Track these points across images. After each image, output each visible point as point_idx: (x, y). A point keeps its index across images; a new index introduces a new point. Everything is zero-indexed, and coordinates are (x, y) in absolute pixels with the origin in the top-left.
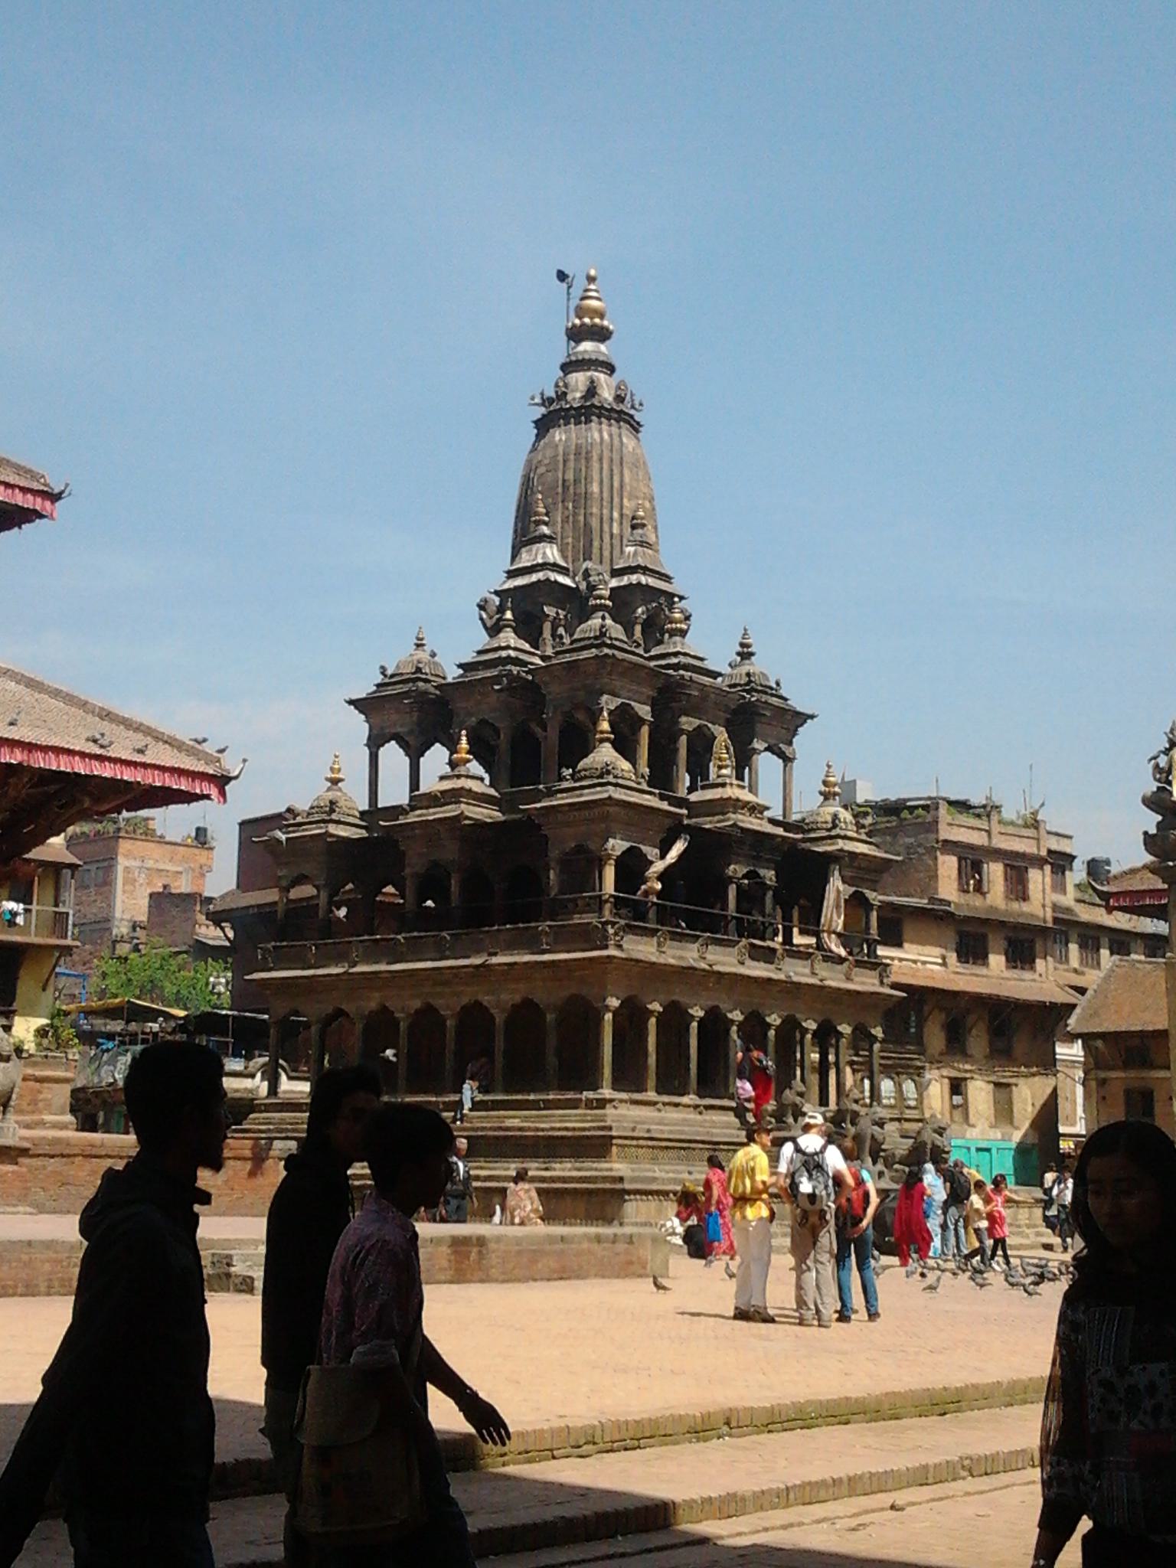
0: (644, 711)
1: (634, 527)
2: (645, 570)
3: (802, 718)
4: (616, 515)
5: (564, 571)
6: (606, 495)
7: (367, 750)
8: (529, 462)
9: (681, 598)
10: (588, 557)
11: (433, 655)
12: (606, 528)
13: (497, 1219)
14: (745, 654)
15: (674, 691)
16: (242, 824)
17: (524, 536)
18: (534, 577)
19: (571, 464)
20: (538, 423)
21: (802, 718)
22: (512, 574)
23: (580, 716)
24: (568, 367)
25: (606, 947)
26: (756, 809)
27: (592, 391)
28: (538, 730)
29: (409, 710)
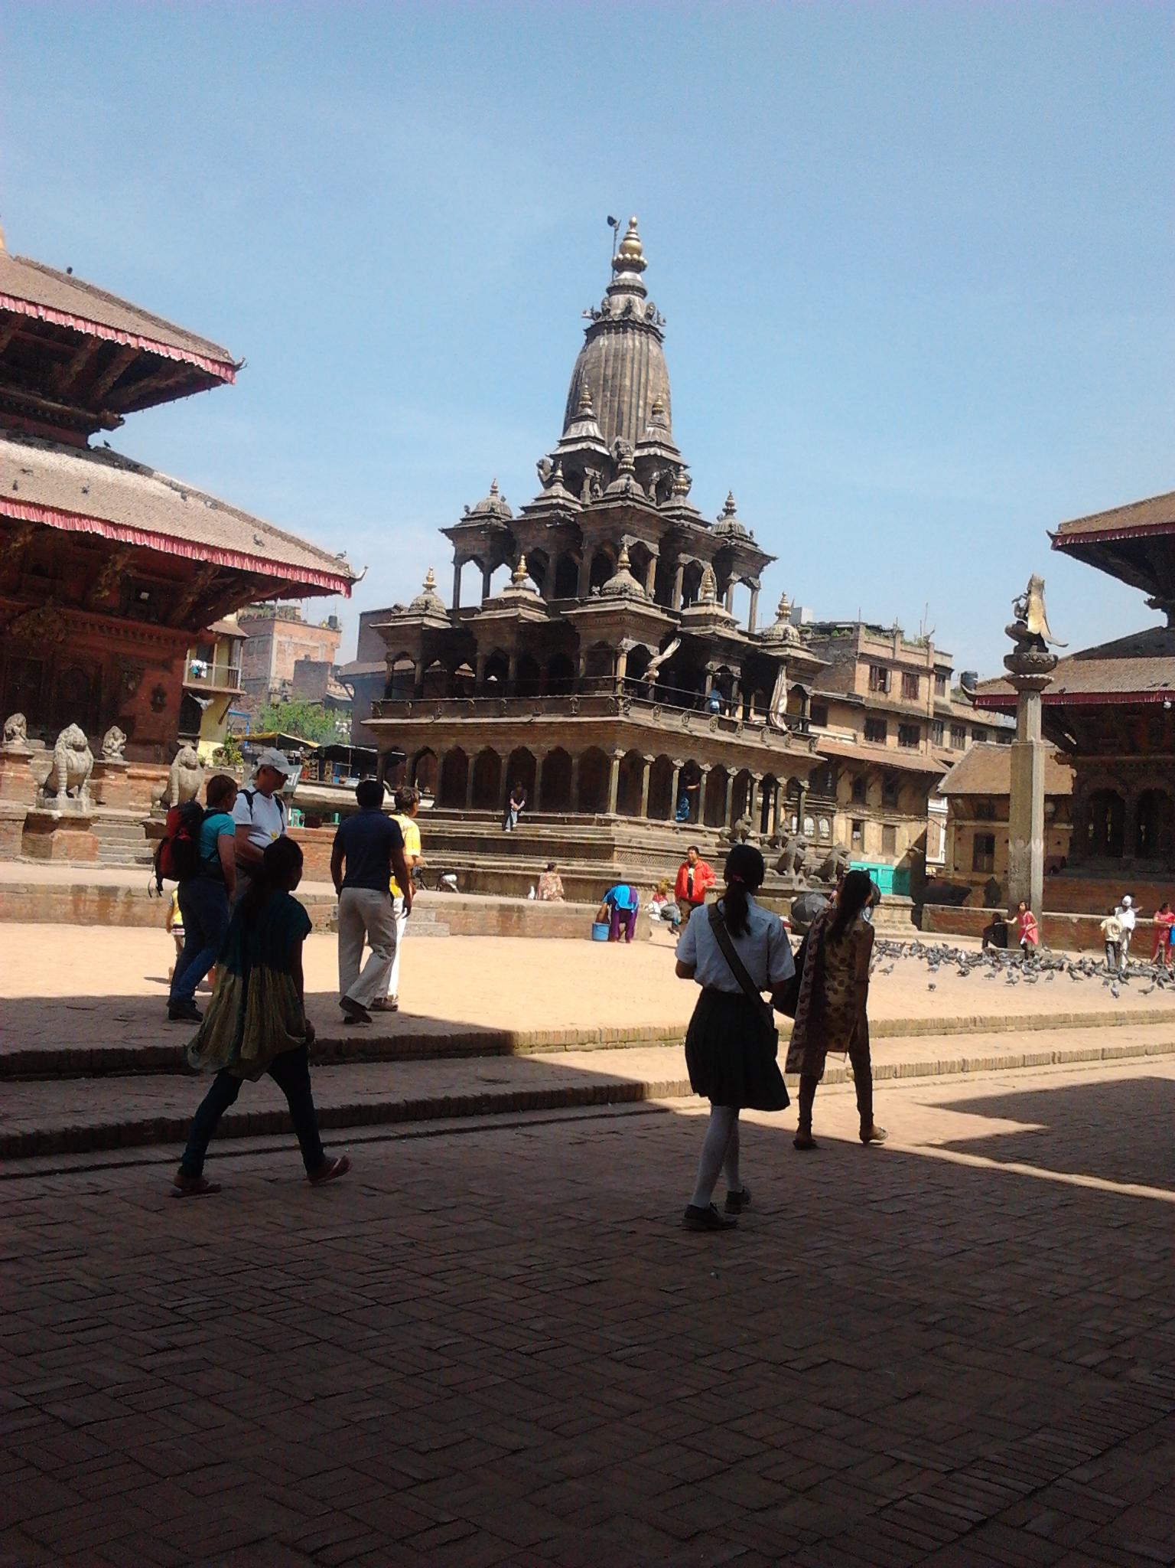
0: (654, 548)
1: (654, 413)
2: (660, 445)
3: (767, 559)
4: (641, 403)
5: (601, 442)
6: (635, 388)
7: (453, 567)
8: (579, 361)
9: (686, 467)
10: (619, 433)
11: (503, 499)
12: (634, 412)
13: (532, 894)
14: (729, 511)
15: (676, 535)
16: (363, 615)
17: (574, 415)
18: (579, 446)
19: (611, 363)
20: (588, 331)
21: (767, 559)
22: (563, 443)
23: (608, 550)
24: (612, 290)
25: (617, 715)
26: (730, 623)
27: (629, 309)
28: (577, 558)
29: (485, 539)
